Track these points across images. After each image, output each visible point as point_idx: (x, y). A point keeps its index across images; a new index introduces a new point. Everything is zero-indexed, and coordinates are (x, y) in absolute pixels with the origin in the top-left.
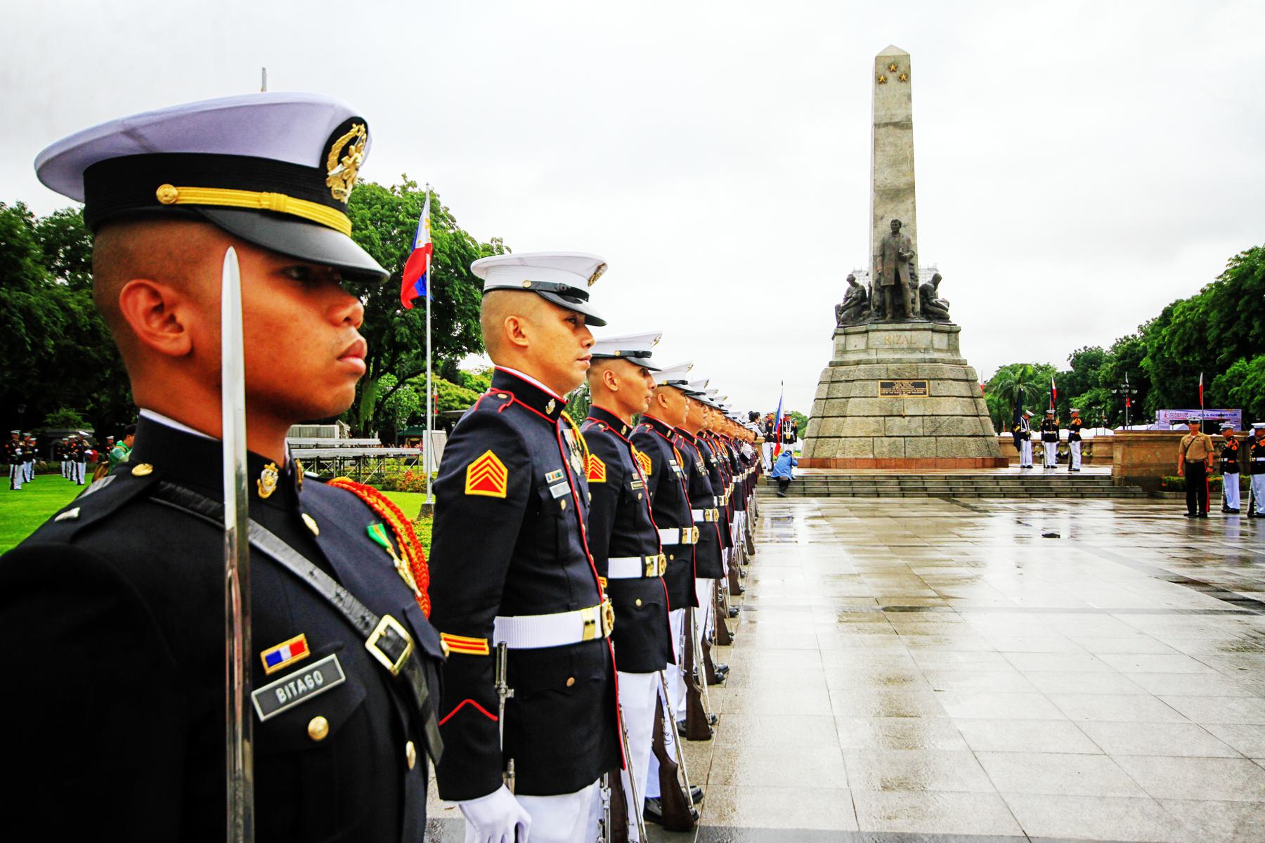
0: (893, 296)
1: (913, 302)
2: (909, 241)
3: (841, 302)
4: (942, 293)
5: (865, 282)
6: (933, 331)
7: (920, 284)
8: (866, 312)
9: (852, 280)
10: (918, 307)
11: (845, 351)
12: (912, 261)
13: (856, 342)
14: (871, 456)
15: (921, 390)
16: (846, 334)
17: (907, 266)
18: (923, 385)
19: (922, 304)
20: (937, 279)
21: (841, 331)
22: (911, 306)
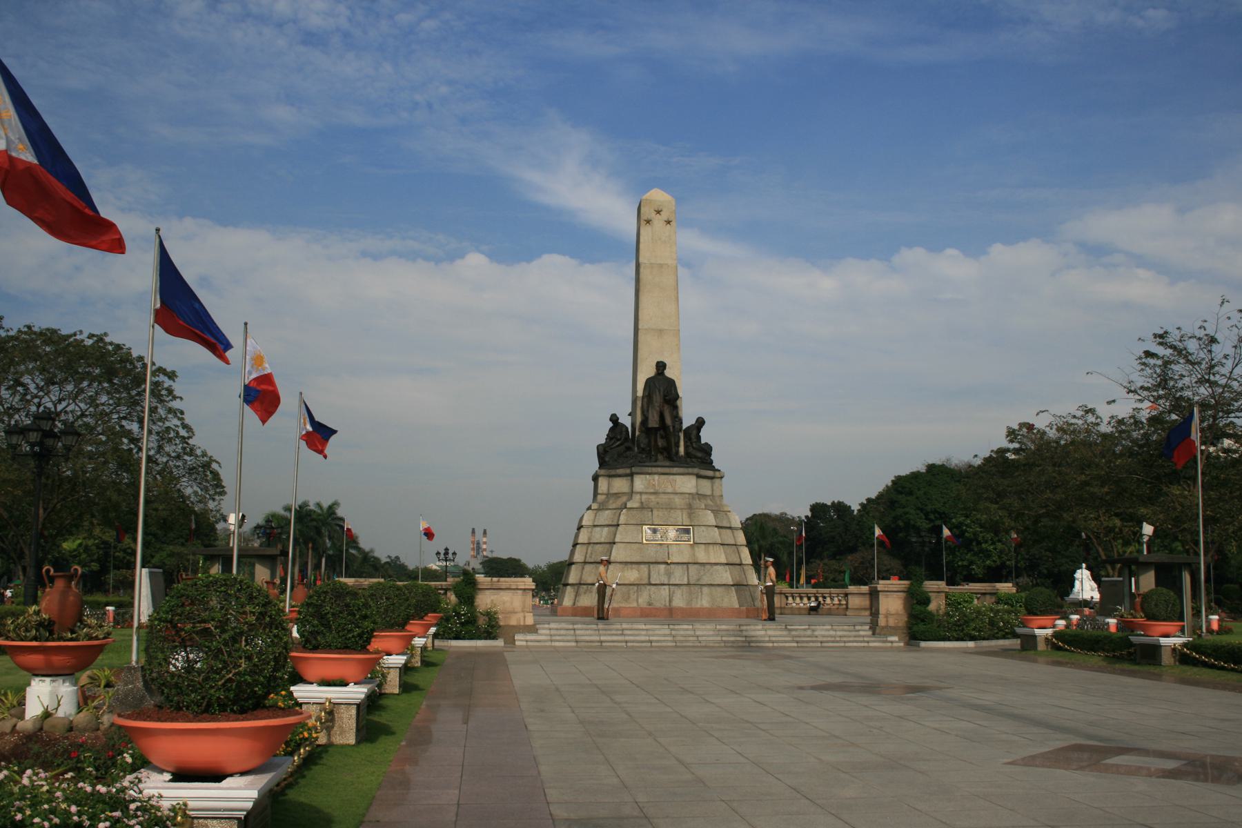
0: (657, 437)
1: (677, 445)
4: (706, 436)
6: (699, 476)
9: (614, 419)
10: (682, 450)
14: (635, 605)
16: (610, 476)
19: (686, 447)
20: (700, 423)
21: (602, 472)
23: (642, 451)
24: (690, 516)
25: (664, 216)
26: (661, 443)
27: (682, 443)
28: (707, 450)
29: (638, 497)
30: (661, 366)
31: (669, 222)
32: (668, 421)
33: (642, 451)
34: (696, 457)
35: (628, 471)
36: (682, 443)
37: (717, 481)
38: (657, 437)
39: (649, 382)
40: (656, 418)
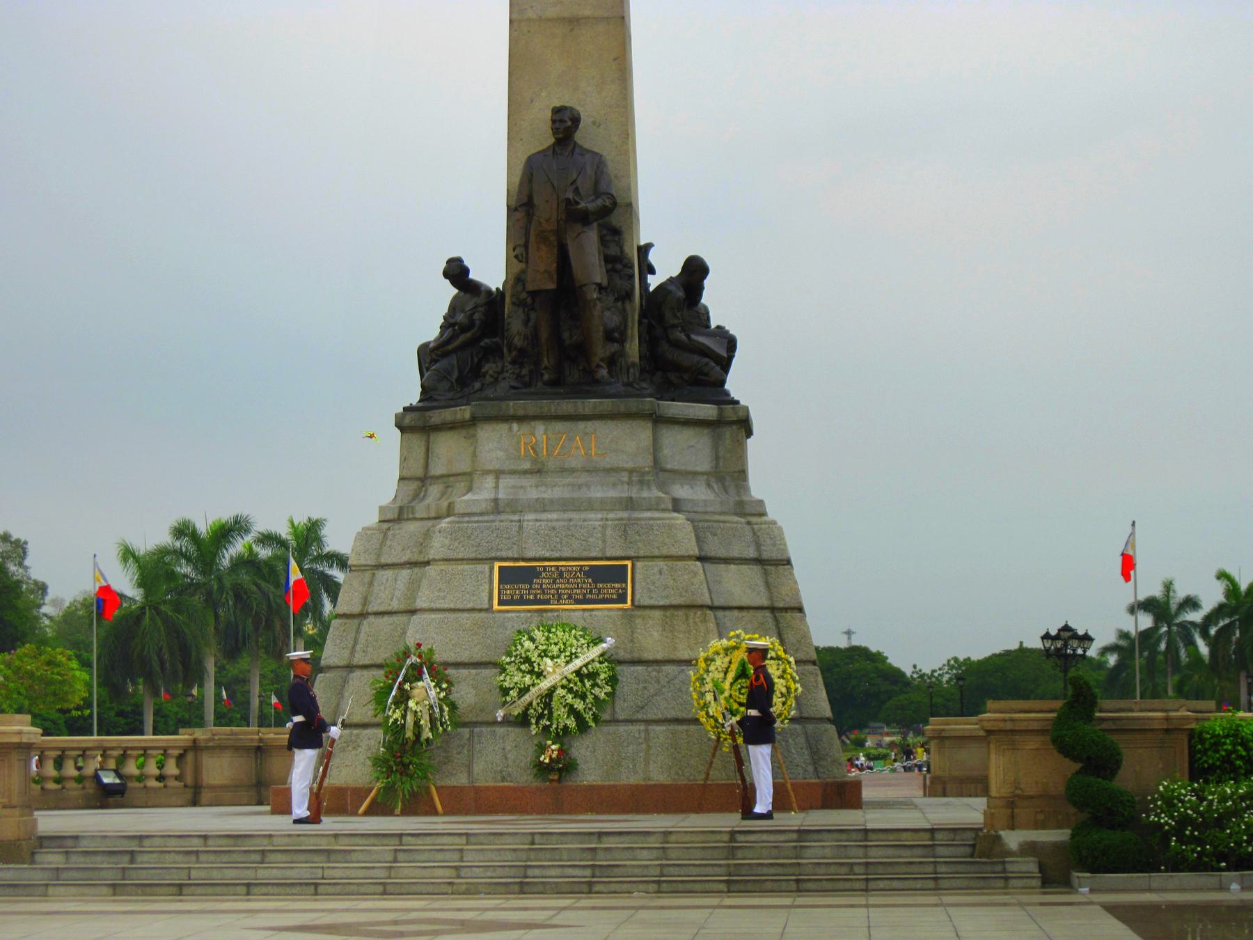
1: (615, 336)
2: (599, 163)
3: (431, 332)
4: (720, 302)
5: (491, 271)
6: (658, 420)
7: (654, 282)
8: (489, 368)
9: (456, 272)
10: (633, 349)
11: (425, 480)
12: (615, 219)
13: (449, 451)
17: (591, 237)
18: (618, 574)
19: (650, 340)
20: (695, 271)
22: (601, 351)
23: (521, 357)
24: (624, 529)
27: (634, 332)
29: (489, 481)
30: (565, 124)
34: (677, 368)
35: (464, 412)
37: (728, 433)
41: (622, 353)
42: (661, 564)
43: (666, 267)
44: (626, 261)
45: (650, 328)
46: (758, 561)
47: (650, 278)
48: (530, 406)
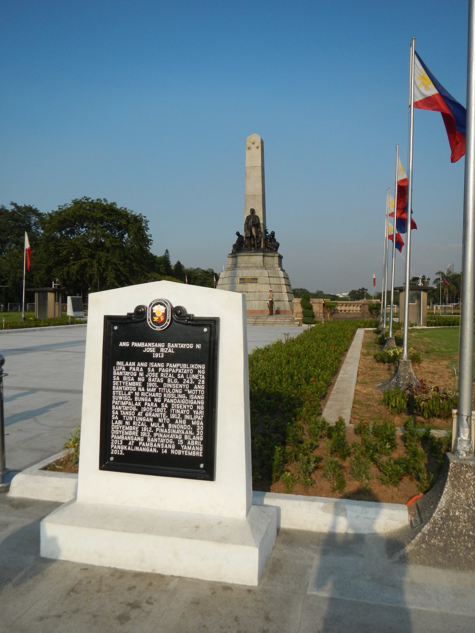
3: (235, 242)
9: (238, 234)
10: (262, 246)
15: (255, 281)
18: (257, 279)
20: (273, 234)
23: (246, 246)
25: (256, 145)
26: (252, 242)
27: (262, 243)
28: (277, 246)
30: (253, 211)
31: (258, 148)
32: (254, 233)
33: (246, 246)
36: (262, 243)
38: (256, 239)
39: (248, 218)
40: (249, 233)
41: (260, 246)
42: (263, 277)
43: (270, 233)
44: (266, 232)
45: (265, 242)
46: (279, 277)
47: (267, 234)
48: (245, 254)
